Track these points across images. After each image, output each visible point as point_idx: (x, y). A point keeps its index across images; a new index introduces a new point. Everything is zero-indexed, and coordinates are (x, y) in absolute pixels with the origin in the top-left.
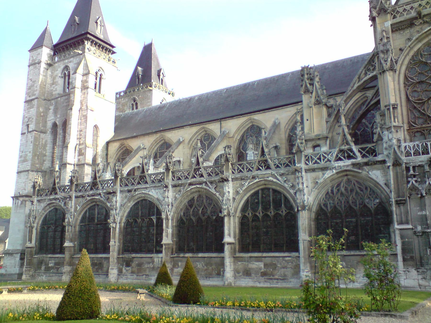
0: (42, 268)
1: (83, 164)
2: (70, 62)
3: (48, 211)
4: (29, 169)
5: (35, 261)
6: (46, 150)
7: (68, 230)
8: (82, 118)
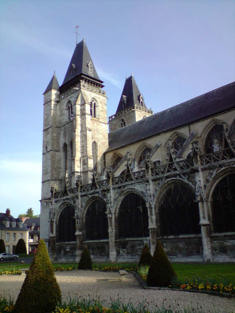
1: (87, 171)
2: (72, 97)
3: (63, 209)
4: (50, 179)
5: (57, 247)
6: (60, 164)
7: (77, 222)
8: (83, 137)
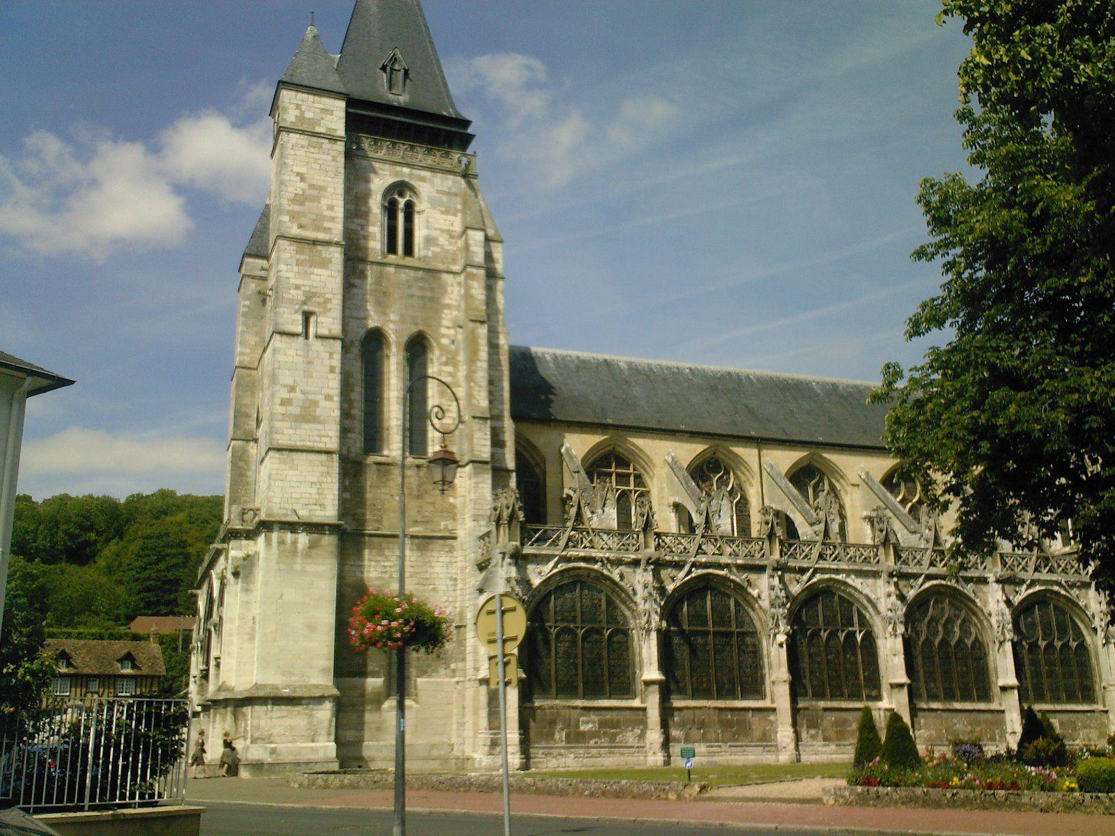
0: (557, 736)
2: (423, 179)
